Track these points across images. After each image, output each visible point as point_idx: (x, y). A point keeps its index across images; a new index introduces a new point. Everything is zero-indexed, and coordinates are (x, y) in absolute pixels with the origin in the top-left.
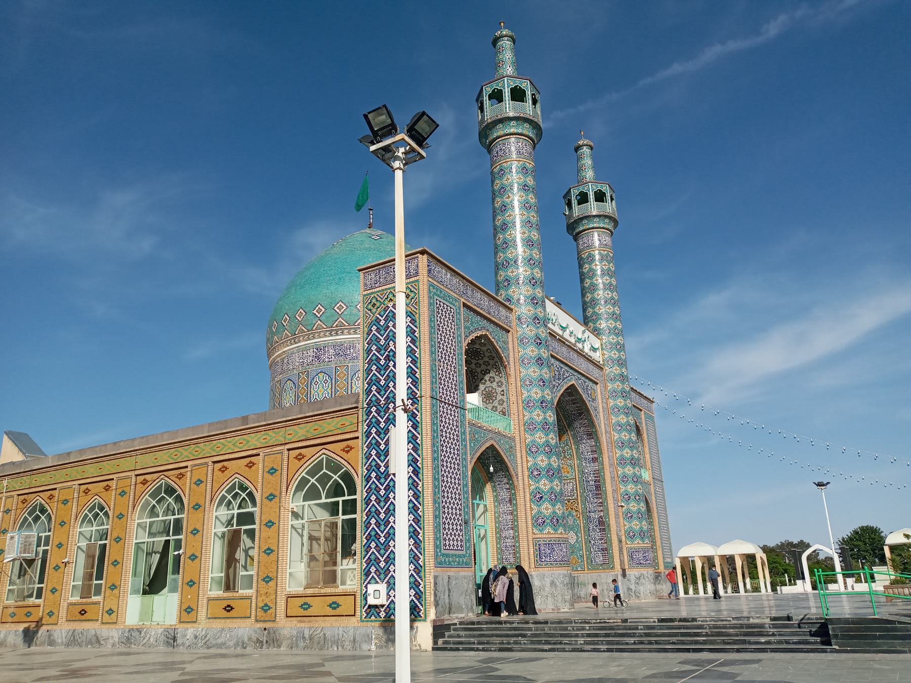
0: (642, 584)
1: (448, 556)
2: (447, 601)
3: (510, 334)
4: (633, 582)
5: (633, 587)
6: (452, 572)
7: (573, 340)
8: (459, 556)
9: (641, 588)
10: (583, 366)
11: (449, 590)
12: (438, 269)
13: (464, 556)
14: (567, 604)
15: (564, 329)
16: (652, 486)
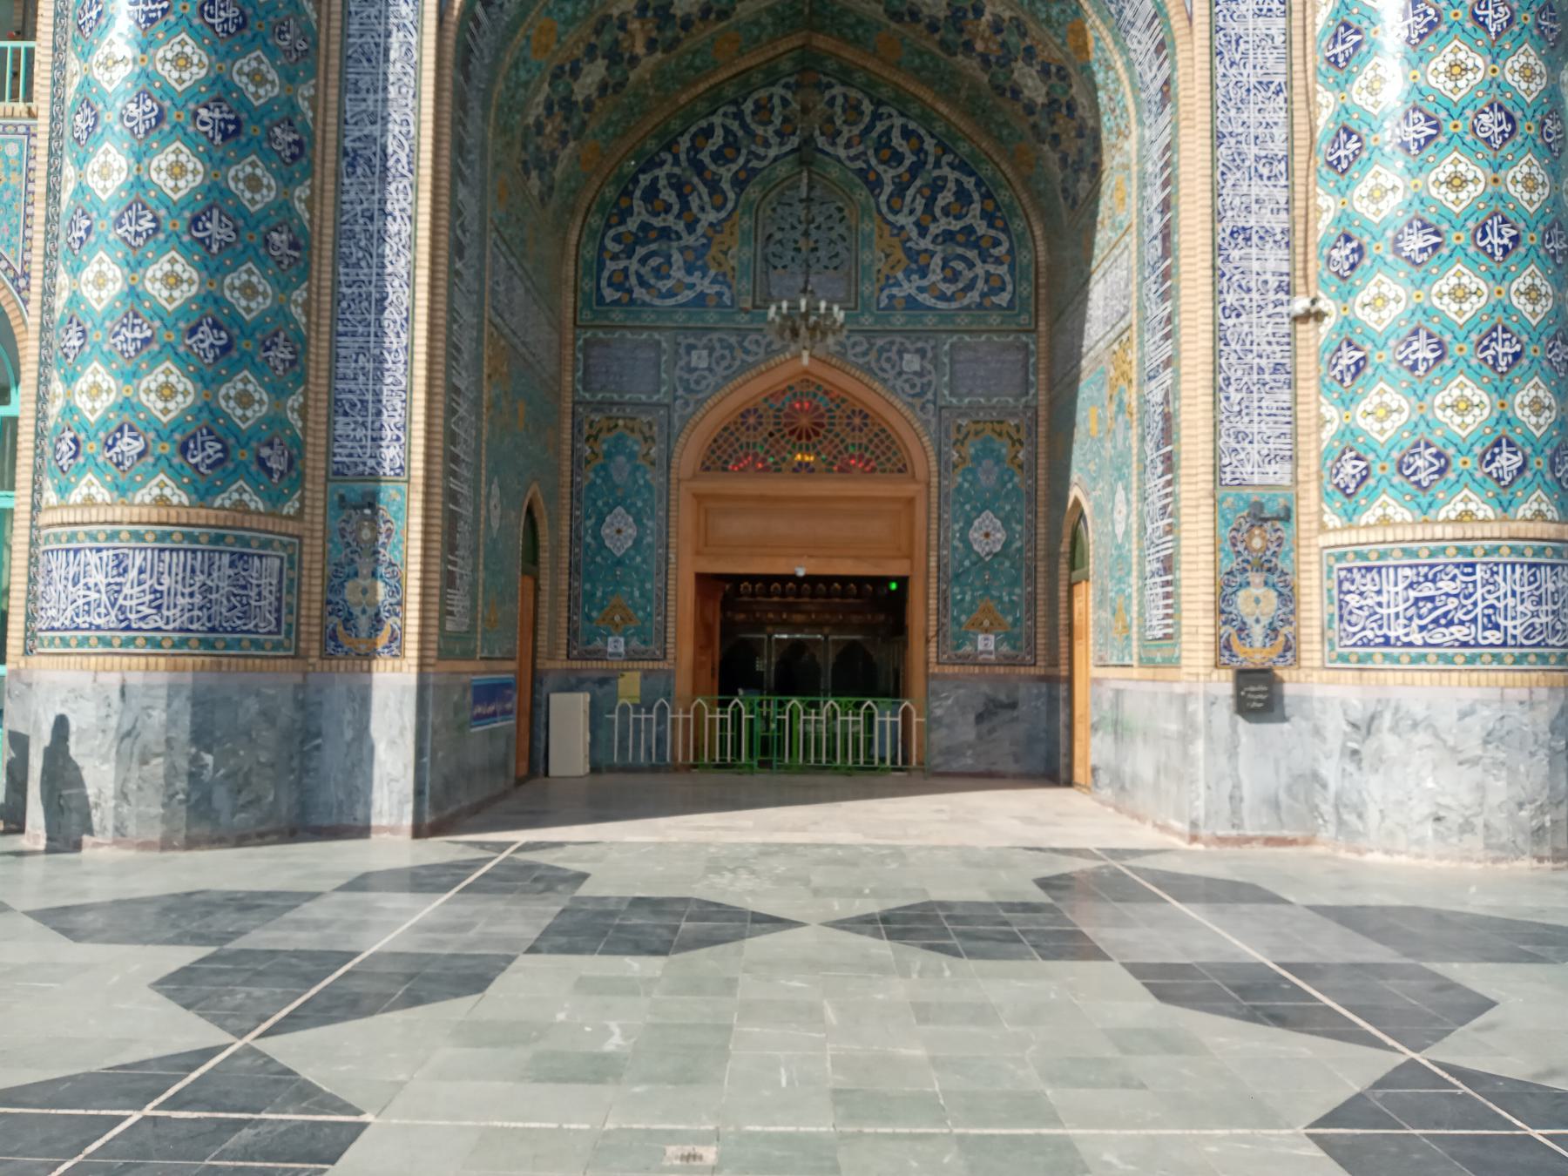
0: (1380, 759)
4: (1334, 743)
5: (1330, 771)
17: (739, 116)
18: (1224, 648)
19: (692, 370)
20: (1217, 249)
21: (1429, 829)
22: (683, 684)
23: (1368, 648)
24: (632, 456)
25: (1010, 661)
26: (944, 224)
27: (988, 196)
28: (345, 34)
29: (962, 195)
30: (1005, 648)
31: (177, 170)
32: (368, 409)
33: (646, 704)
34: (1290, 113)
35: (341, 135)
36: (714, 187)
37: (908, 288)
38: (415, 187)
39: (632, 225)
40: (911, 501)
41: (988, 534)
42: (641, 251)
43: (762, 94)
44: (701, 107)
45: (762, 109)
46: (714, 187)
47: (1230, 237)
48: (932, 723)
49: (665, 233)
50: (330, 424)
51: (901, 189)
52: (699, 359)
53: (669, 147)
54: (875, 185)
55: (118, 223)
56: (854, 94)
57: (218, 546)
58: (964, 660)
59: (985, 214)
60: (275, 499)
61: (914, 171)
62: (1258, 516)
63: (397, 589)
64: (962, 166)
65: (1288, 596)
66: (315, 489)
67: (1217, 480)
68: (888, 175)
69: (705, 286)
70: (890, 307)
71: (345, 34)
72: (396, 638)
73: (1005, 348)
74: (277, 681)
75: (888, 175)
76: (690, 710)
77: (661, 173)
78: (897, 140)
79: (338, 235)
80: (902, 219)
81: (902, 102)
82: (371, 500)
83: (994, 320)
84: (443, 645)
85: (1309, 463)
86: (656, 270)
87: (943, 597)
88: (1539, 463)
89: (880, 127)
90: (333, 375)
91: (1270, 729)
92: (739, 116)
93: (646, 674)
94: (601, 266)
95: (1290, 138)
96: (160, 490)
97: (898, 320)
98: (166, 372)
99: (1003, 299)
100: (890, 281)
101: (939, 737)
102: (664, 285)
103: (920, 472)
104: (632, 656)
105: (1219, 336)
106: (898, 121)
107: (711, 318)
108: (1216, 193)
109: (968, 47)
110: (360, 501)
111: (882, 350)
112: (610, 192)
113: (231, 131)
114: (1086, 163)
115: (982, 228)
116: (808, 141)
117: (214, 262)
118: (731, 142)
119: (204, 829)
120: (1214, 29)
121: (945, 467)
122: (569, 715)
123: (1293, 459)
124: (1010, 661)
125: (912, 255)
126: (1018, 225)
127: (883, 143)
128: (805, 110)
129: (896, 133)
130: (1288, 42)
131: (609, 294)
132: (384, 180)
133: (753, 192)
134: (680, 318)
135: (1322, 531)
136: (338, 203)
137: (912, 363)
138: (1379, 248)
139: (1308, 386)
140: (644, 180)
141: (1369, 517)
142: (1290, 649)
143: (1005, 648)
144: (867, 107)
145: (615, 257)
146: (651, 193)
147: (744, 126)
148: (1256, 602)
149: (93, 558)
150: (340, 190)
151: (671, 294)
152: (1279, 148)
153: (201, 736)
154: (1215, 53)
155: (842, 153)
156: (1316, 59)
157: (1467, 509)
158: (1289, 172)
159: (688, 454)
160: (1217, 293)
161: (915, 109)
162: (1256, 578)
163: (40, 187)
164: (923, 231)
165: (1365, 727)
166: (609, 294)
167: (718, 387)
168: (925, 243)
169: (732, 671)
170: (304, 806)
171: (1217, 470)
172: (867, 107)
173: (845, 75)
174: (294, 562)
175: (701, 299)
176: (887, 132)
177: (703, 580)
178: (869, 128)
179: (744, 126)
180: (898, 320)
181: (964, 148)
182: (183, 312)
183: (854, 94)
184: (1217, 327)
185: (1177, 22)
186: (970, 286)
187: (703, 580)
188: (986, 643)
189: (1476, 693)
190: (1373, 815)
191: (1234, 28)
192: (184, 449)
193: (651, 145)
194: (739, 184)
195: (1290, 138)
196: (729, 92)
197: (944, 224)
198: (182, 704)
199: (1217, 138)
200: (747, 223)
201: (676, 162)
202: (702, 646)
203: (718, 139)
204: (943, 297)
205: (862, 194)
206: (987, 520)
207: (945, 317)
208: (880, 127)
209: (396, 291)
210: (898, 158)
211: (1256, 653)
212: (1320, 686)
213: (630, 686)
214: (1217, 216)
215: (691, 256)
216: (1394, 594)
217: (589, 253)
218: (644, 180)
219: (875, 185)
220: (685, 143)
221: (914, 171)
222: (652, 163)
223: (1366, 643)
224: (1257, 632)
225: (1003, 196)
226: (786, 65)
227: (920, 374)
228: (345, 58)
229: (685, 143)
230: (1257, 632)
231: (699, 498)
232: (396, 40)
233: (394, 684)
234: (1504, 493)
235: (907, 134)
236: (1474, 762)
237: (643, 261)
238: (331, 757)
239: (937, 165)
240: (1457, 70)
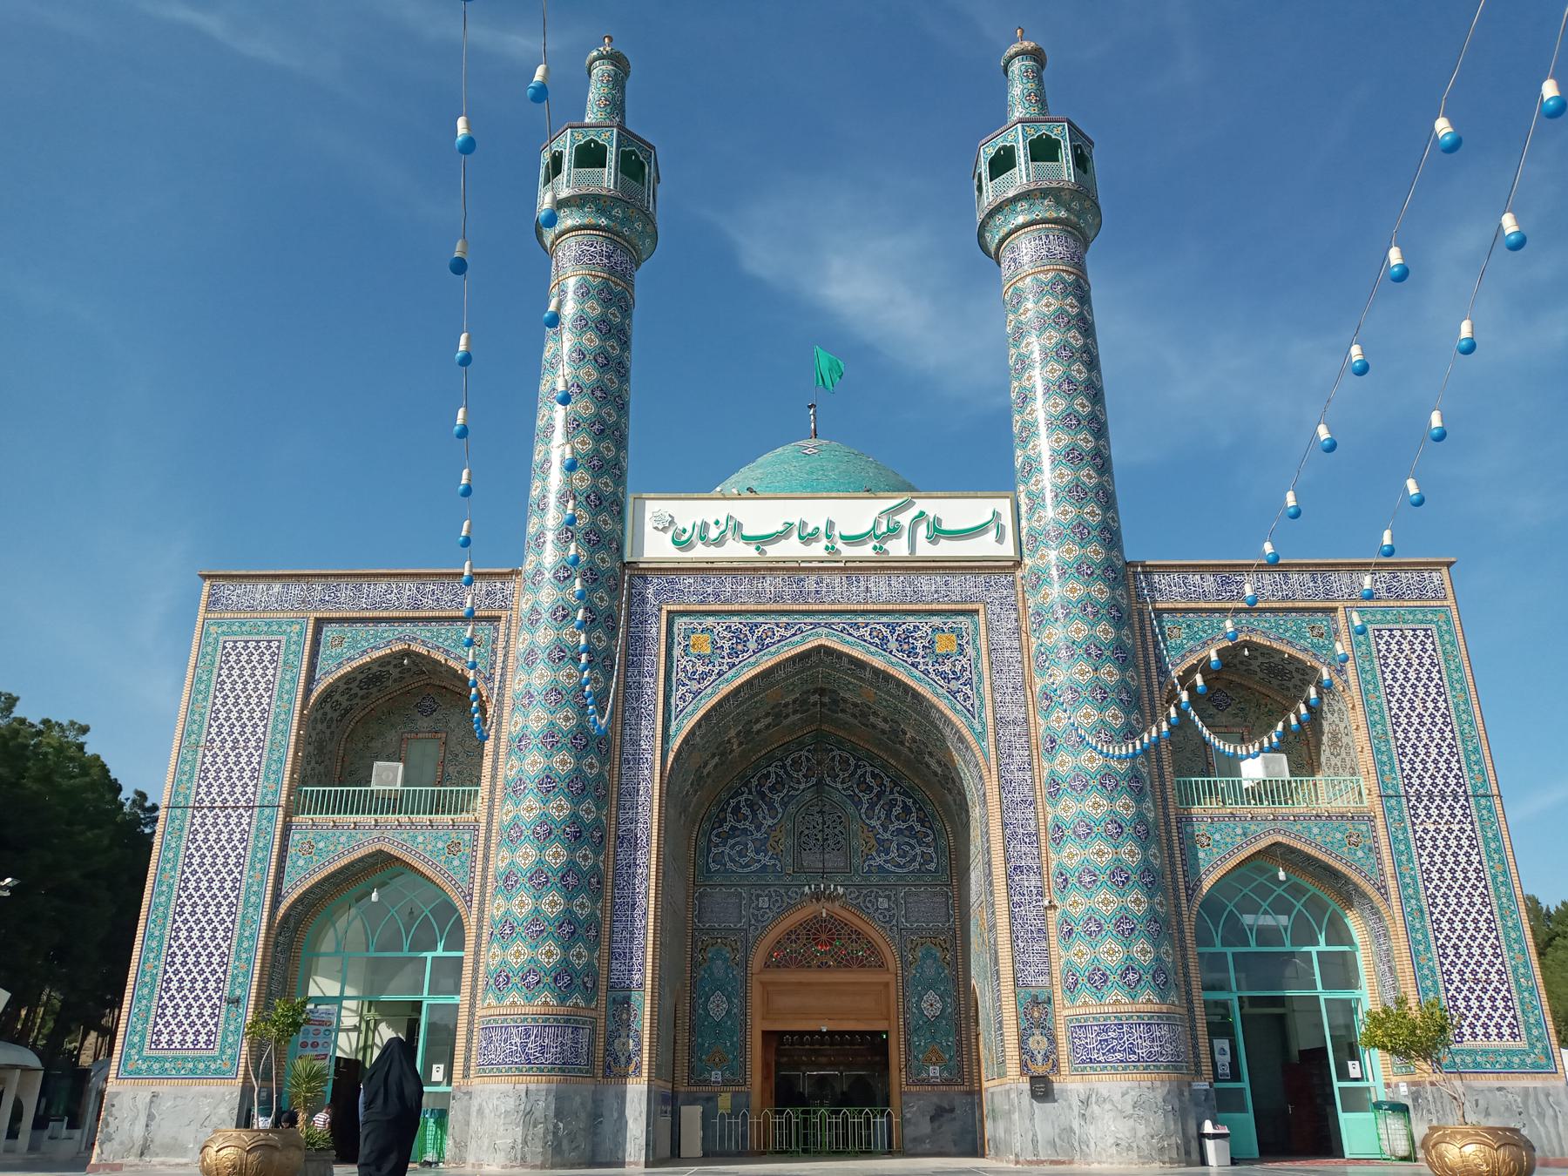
1: (157, 1060)
2: (139, 1131)
3: (502, 625)
5: (1076, 1126)
6: (164, 1088)
7: (818, 550)
8: (200, 1059)
9: (1092, 1130)
10: (882, 590)
11: (151, 1117)
12: (233, 593)
13: (214, 1059)
14: (501, 1158)
15: (762, 541)
16: (1379, 822)
17: (783, 767)
18: (1024, 1066)
19: (759, 909)
20: (1008, 876)
21: (1114, 1150)
22: (756, 1099)
23: (1086, 1063)
24: (726, 960)
25: (948, 1083)
26: (897, 825)
27: (920, 809)
28: (620, 783)
29: (906, 809)
30: (945, 1074)
31: (556, 855)
32: (627, 956)
33: (734, 1112)
34: (1036, 814)
35: (617, 829)
36: (771, 807)
37: (879, 861)
38: (649, 852)
39: (726, 827)
40: (887, 985)
41: (931, 1004)
42: (731, 842)
43: (796, 755)
44: (763, 763)
46: (771, 807)
47: (1014, 871)
48: (904, 1122)
50: (610, 964)
51: (872, 807)
52: (764, 903)
54: (858, 803)
55: (531, 879)
56: (845, 754)
57: (570, 1023)
58: (922, 1082)
59: (919, 820)
60: (588, 1001)
61: (879, 796)
62: (1036, 1001)
63: (639, 1044)
64: (905, 793)
65: (1052, 1040)
66: (602, 994)
67: (1016, 985)
69: (766, 860)
70: (869, 871)
71: (620, 783)
72: (638, 1067)
73: (935, 894)
74: (587, 1087)
76: (759, 1111)
77: (742, 799)
78: (869, 779)
79: (614, 875)
80: (873, 823)
81: (871, 758)
82: (627, 1000)
83: (928, 879)
84: (657, 1072)
85: (1057, 974)
86: (739, 853)
87: (908, 1043)
88: (1147, 977)
89: (859, 772)
90: (611, 941)
91: (1048, 1106)
92: (783, 767)
93: (734, 1095)
94: (709, 851)
95: (1037, 825)
96: (545, 1000)
97: (874, 879)
98: (550, 945)
99: (932, 867)
100: (869, 857)
101: (910, 1131)
102: (743, 861)
103: (891, 966)
104: (726, 1083)
105: (1012, 916)
106: (869, 769)
107: (771, 879)
108: (1006, 850)
109: (902, 743)
110: (622, 1002)
111: (866, 896)
112: (714, 810)
113: (577, 836)
114: (964, 808)
115: (918, 827)
116: (820, 782)
117: (570, 893)
119: (558, 1159)
120: (1000, 777)
121: (906, 965)
122: (692, 1115)
123: (1050, 974)
124: (948, 1083)
125: (880, 842)
126: (937, 825)
127: (862, 782)
128: (819, 763)
129: (868, 776)
130: (1033, 782)
132: (636, 850)
133: (792, 809)
134: (753, 880)
135: (1065, 1011)
136: (615, 860)
137: (883, 903)
138: (1073, 880)
139: (1054, 940)
140: (733, 802)
141: (1079, 1003)
142: (1056, 1065)
143: (945, 1074)
144: (852, 762)
145: (717, 846)
147: (786, 772)
148: (1038, 1043)
149: (514, 1031)
150: (616, 854)
151: (747, 865)
152: (1032, 829)
153: (559, 1114)
154: (1001, 787)
155: (839, 786)
156: (1045, 791)
157: (1116, 1002)
158: (1038, 841)
159: (757, 962)
160: (1009, 896)
161: (878, 762)
162: (1037, 1032)
163: (480, 855)
164: (885, 829)
165: (1086, 1103)
167: (774, 918)
168: (887, 836)
169: (784, 1094)
170: (594, 1153)
171: (1015, 979)
172: (852, 762)
173: (840, 744)
174: (594, 1031)
176: (864, 775)
177: (765, 1033)
178: (855, 772)
179: (786, 772)
181: (905, 784)
182: (557, 918)
183: (845, 754)
184: (1011, 912)
185: (985, 773)
186: (913, 860)
187: (765, 1033)
188: (934, 1071)
189: (1128, 1084)
190: (1092, 1145)
191: (1009, 776)
192: (555, 980)
193: (737, 784)
195: (1037, 825)
196: (778, 754)
197: (897, 825)
198: (551, 1098)
199: (1004, 825)
201: (750, 793)
202: (765, 1078)
204: (899, 866)
205: (851, 809)
206: (931, 996)
207: (901, 878)
208: (859, 772)
209: (640, 900)
210: (870, 789)
211: (1039, 1069)
212: (1070, 1084)
213: (724, 1102)
214: (1007, 860)
215: (758, 844)
216: (1092, 1039)
217: (703, 843)
218: (733, 802)
219: (858, 803)
220: (754, 782)
221: (879, 796)
222: (737, 794)
223: (1083, 1062)
224: (1039, 1058)
225: (929, 809)
226: (808, 739)
227: (888, 910)
228: (619, 794)
229: (754, 782)
230: (1039, 1058)
231: (763, 984)
232: (642, 785)
233: (637, 1091)
234: (1132, 989)
235: (874, 776)
236: (1130, 1116)
237: (732, 848)
238: (607, 1127)
239: (892, 792)
240: (1096, 805)
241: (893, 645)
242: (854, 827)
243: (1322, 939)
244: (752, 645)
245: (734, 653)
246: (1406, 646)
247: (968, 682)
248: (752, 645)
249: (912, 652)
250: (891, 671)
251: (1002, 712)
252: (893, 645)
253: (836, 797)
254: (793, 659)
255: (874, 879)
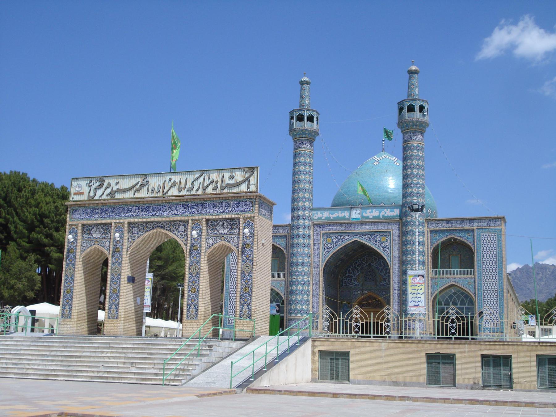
36: (358, 271)
45: (364, 259)
46: (358, 271)
49: (351, 276)
53: (352, 265)
68: (380, 268)
75: (380, 268)
105: (393, 300)
107: (357, 288)
116: (370, 265)
118: (360, 264)
131: (344, 285)
146: (349, 271)
166: (344, 285)
175: (356, 285)
180: (382, 287)
194: (360, 269)
200: (362, 275)
203: (358, 263)
205: (377, 271)
219: (378, 269)
241: (372, 240)
242: (378, 275)
243: (467, 304)
244: (340, 240)
245: (336, 242)
246: (489, 238)
247: (388, 248)
248: (340, 240)
249: (376, 241)
250: (371, 246)
251: (394, 255)
252: (372, 240)
253: (373, 268)
254: (351, 243)
255: (382, 287)
